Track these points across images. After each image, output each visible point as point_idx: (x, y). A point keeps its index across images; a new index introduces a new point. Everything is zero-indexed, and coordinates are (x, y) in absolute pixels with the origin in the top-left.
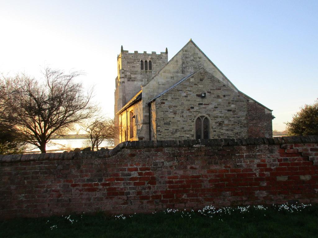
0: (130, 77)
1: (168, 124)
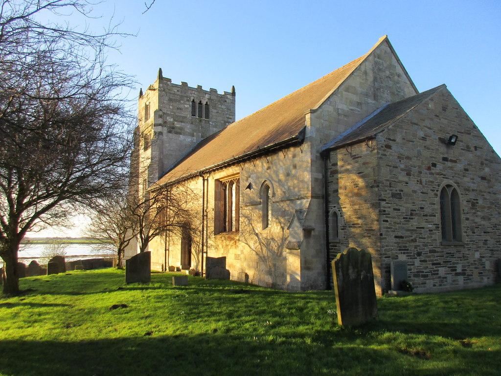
0: (172, 126)
1: (397, 196)
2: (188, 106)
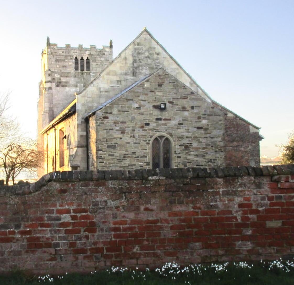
0: (59, 81)
1: (114, 147)
2: (72, 63)
